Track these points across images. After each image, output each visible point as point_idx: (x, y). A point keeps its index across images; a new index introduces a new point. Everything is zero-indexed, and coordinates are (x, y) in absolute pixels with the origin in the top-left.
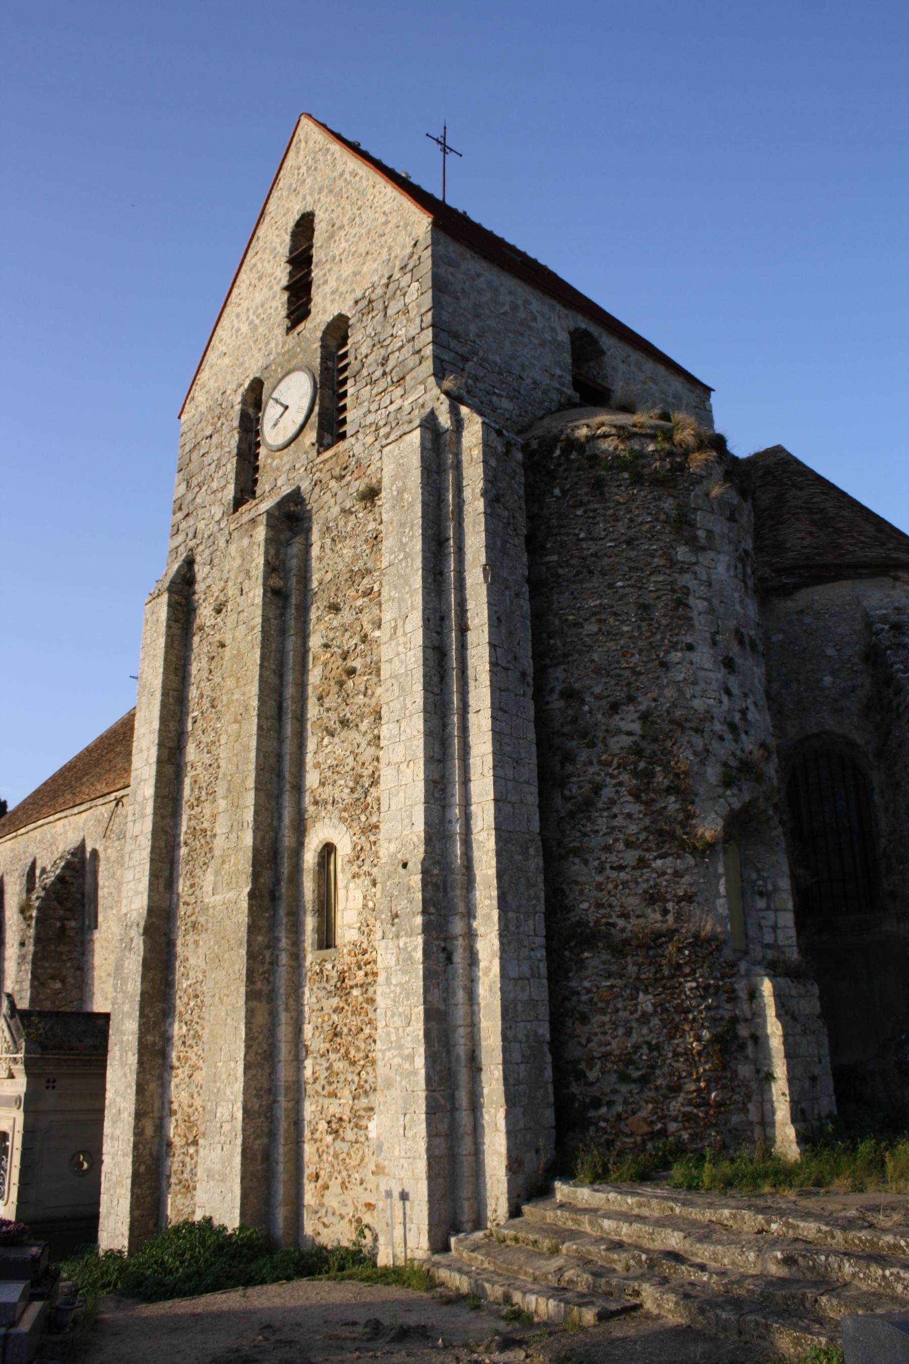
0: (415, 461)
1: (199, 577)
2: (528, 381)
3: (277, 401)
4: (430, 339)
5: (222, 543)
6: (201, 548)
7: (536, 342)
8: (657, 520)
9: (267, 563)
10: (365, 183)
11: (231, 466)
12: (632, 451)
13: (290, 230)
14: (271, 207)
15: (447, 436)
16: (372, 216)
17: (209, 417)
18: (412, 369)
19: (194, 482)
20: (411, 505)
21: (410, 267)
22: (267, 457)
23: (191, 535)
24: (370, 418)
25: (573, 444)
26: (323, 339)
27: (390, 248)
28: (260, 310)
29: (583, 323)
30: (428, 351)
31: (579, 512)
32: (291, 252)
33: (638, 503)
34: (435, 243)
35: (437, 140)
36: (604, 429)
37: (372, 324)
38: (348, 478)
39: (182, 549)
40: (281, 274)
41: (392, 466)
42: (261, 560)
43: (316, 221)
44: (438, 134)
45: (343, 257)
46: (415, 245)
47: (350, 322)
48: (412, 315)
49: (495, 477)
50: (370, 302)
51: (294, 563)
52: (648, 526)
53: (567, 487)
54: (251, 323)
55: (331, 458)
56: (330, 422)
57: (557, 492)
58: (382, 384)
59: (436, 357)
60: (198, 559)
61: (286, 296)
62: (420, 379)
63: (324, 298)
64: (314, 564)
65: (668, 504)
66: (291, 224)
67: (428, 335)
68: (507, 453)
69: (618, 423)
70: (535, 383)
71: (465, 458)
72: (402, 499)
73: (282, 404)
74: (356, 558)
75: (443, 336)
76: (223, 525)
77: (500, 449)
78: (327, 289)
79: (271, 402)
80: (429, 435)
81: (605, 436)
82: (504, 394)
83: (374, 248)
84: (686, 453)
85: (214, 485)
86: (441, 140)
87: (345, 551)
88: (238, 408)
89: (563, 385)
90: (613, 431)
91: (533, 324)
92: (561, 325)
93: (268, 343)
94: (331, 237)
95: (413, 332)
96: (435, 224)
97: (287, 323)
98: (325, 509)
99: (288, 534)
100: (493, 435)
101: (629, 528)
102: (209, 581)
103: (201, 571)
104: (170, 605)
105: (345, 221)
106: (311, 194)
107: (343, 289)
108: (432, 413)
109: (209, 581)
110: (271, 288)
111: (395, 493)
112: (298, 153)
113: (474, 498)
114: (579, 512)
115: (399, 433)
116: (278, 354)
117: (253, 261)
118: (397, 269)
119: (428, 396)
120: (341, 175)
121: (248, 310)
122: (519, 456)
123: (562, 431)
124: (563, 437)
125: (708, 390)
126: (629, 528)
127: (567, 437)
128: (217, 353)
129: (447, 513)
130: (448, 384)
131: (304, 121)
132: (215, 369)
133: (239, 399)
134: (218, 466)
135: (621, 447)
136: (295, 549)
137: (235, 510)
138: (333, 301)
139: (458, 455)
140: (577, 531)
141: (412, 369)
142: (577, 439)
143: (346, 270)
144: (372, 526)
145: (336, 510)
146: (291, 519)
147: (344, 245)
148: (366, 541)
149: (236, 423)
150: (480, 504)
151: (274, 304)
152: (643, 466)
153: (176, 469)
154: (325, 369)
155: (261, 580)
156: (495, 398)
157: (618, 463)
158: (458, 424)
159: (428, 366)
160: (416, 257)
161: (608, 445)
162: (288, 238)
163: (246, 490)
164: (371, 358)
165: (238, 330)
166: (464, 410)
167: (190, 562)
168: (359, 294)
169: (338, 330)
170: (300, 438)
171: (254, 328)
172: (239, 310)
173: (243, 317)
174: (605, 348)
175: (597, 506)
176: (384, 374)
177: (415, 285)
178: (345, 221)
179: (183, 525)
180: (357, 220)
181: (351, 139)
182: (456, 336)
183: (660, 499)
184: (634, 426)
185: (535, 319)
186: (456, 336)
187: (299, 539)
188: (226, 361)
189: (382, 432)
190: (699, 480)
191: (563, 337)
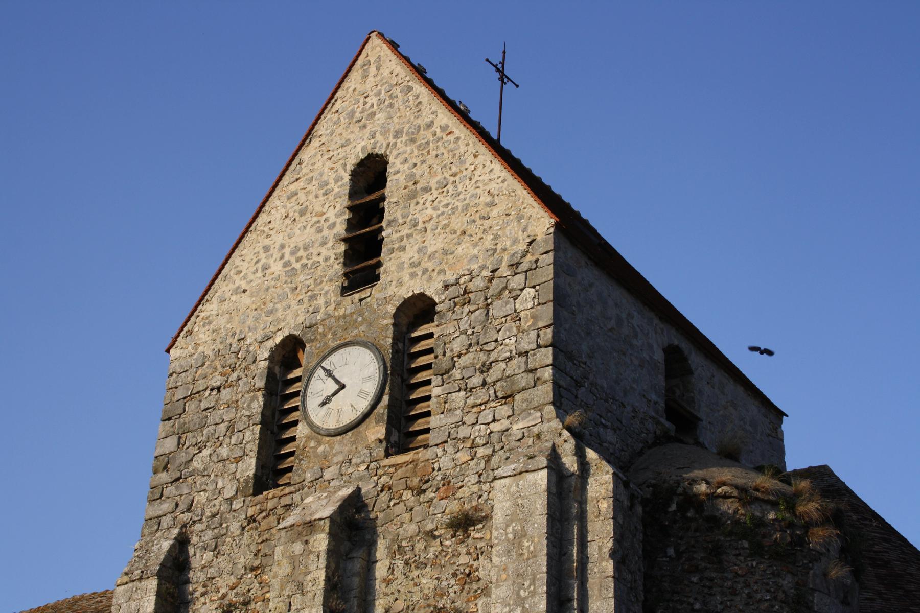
0: (540, 505)
1: (196, 562)
2: (629, 408)
3: (329, 373)
4: (550, 361)
5: (235, 528)
6: (199, 527)
7: (636, 362)
8: (775, 598)
9: (328, 580)
10: (463, 149)
11: (252, 435)
12: (753, 517)
13: (349, 168)
14: (322, 128)
15: (573, 481)
16: (471, 190)
17: (218, 364)
18: (524, 389)
19: (190, 439)
20: (533, 555)
21: (524, 266)
22: (309, 438)
23: (182, 507)
24: (463, 432)
25: (691, 501)
26: (395, 316)
27: (496, 237)
28: (301, 253)
29: (677, 340)
30: (548, 373)
31: (695, 579)
32: (352, 195)
33: (757, 577)
34: (556, 249)
35: (495, 66)
36: (725, 488)
37: (467, 318)
38: (430, 494)
39: (166, 521)
40: (335, 216)
41: (508, 504)
42: (322, 575)
43: (390, 169)
44: (497, 60)
45: (429, 226)
46: (530, 243)
47: (438, 308)
48: (525, 325)
49: (622, 536)
50: (465, 292)
51: (356, 581)
52: (766, 604)
53: (682, 548)
54: (286, 265)
55: (407, 463)
56: (402, 415)
57: (671, 551)
58: (481, 395)
59: (556, 386)
60: (194, 539)
61: (342, 248)
62: (535, 403)
63: (400, 267)
64: (379, 586)
65: (787, 582)
66: (352, 162)
67: (547, 355)
68: (631, 507)
69: (740, 481)
70: (634, 411)
71: (590, 508)
72: (520, 546)
73: (337, 381)
74: (440, 593)
75: (561, 356)
76: (237, 505)
77: (626, 503)
78: (405, 257)
79: (320, 372)
80: (554, 479)
81: (725, 496)
82: (609, 424)
83: (471, 229)
84: (808, 526)
85: (224, 452)
86: (500, 66)
87: (424, 581)
88: (264, 364)
89: (657, 412)
90: (735, 493)
91: (635, 342)
92: (655, 340)
93: (313, 298)
94: (413, 196)
95: (525, 346)
96: (557, 226)
97: (341, 281)
98: (399, 524)
99: (348, 545)
100: (621, 487)
101: (747, 604)
102: (211, 572)
103: (198, 558)
104: (159, 594)
105: (433, 184)
106: (385, 133)
107: (430, 265)
108: (554, 448)
109: (211, 572)
110: (320, 231)
111: (511, 536)
112: (365, 76)
113: (601, 559)
114: (695, 579)
115: (521, 467)
116: (329, 316)
117: (292, 188)
118: (505, 263)
119: (545, 427)
120: (430, 125)
121: (282, 247)
122: (639, 509)
123: (678, 483)
124: (680, 490)
125: (781, 414)
126: (747, 604)
127: (685, 492)
128: (231, 286)
129: (571, 569)
130: (571, 419)
131: (375, 41)
132: (227, 306)
133: (267, 355)
134: (231, 429)
135: (742, 511)
136: (357, 565)
137: (257, 491)
138: (413, 275)
139: (583, 502)
140: (691, 600)
141: (524, 389)
142: (696, 495)
143: (435, 244)
144: (464, 559)
145: (412, 528)
146: (353, 528)
147: (430, 211)
148: (455, 575)
149: (260, 383)
150: (609, 567)
151: (324, 252)
152: (764, 536)
153: (160, 415)
154: (396, 351)
155: (319, 599)
156: (601, 430)
157: (739, 530)
158: (584, 467)
159: (545, 392)
160: (529, 257)
161: (728, 507)
162: (347, 178)
163: (272, 469)
164: (465, 360)
165: (265, 268)
166: (591, 454)
167: (182, 542)
168: (451, 279)
169: (418, 310)
170: (362, 428)
171: (293, 273)
172: (267, 242)
173: (277, 255)
174: (693, 367)
175: (714, 575)
176: (484, 383)
177: (529, 292)
178: (433, 184)
179: (170, 490)
180: (450, 187)
181: (440, 86)
182: (570, 357)
183: (779, 575)
184: (756, 489)
185: (636, 336)
186: (570, 357)
187: (360, 553)
188: (246, 300)
189: (481, 452)
190: (816, 557)
191: (659, 356)
